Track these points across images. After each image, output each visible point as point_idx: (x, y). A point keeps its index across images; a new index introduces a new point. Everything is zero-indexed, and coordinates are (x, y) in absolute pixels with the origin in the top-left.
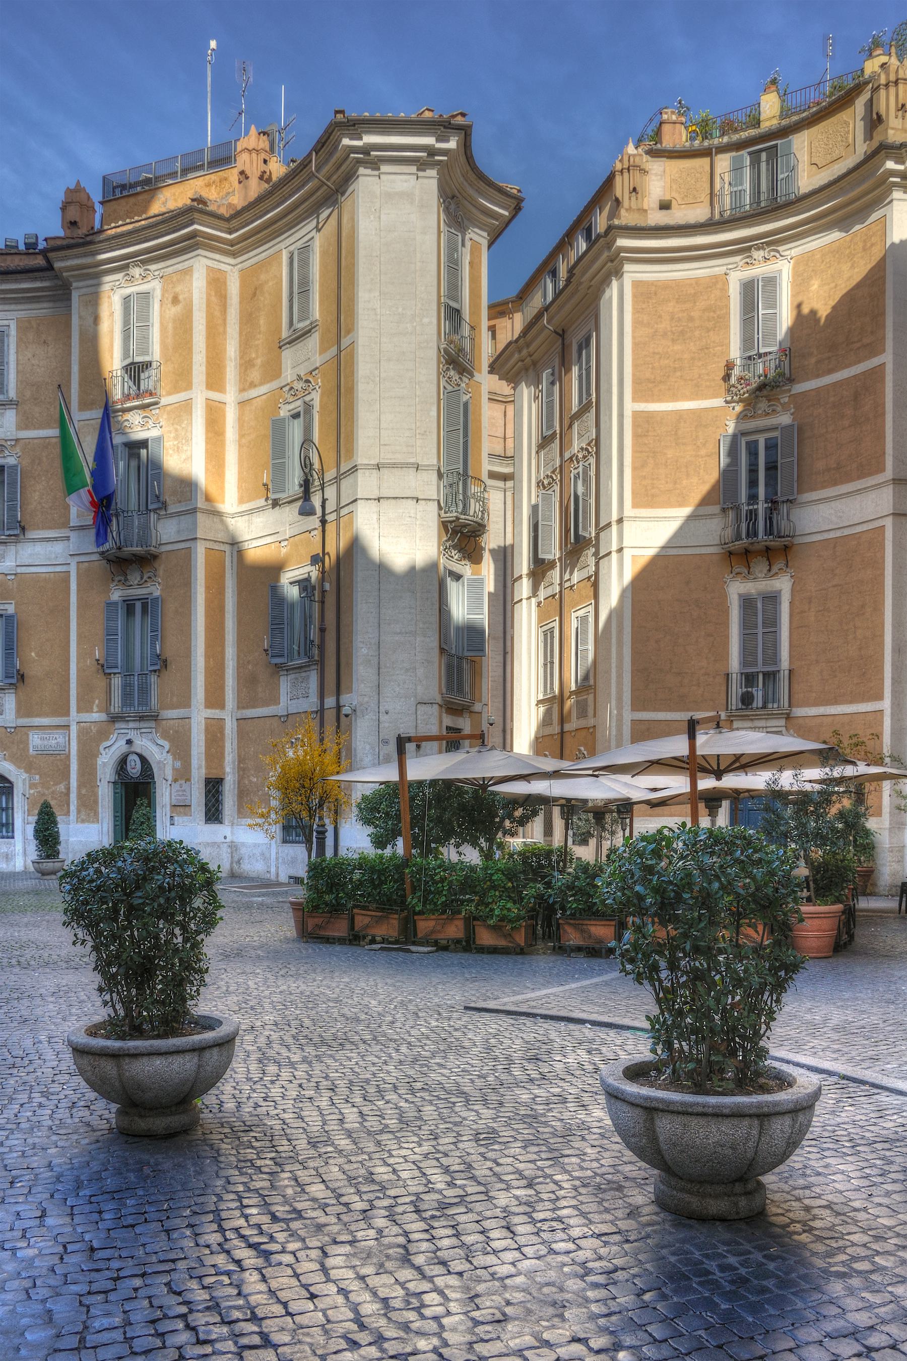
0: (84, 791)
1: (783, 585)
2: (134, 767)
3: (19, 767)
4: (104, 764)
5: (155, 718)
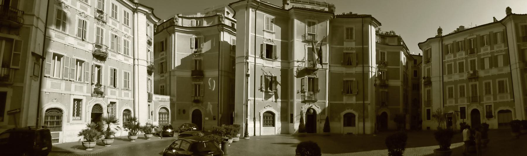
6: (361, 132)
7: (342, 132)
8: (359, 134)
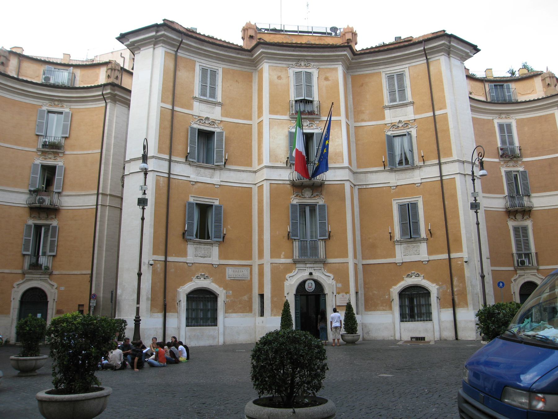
0: (275, 299)
1: (528, 223)
2: (310, 287)
3: (220, 287)
4: (291, 285)
5: (324, 263)
6: (449, 334)
7: (397, 337)
8: (442, 341)
